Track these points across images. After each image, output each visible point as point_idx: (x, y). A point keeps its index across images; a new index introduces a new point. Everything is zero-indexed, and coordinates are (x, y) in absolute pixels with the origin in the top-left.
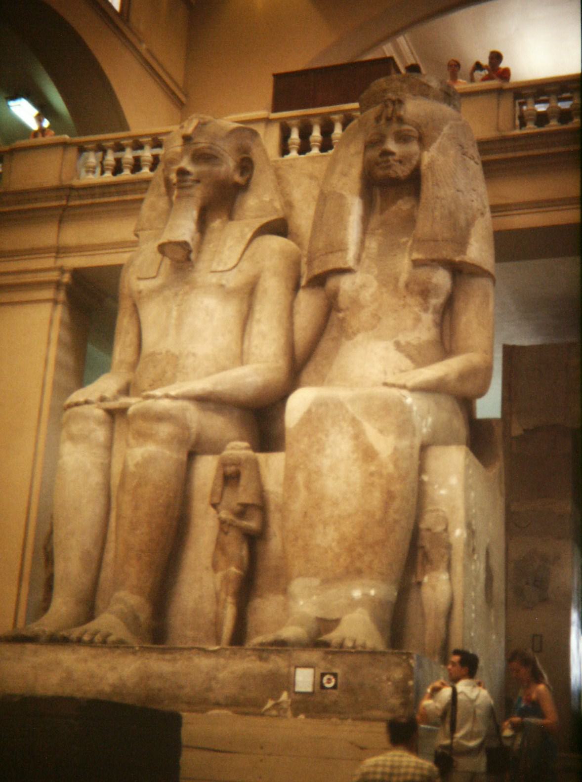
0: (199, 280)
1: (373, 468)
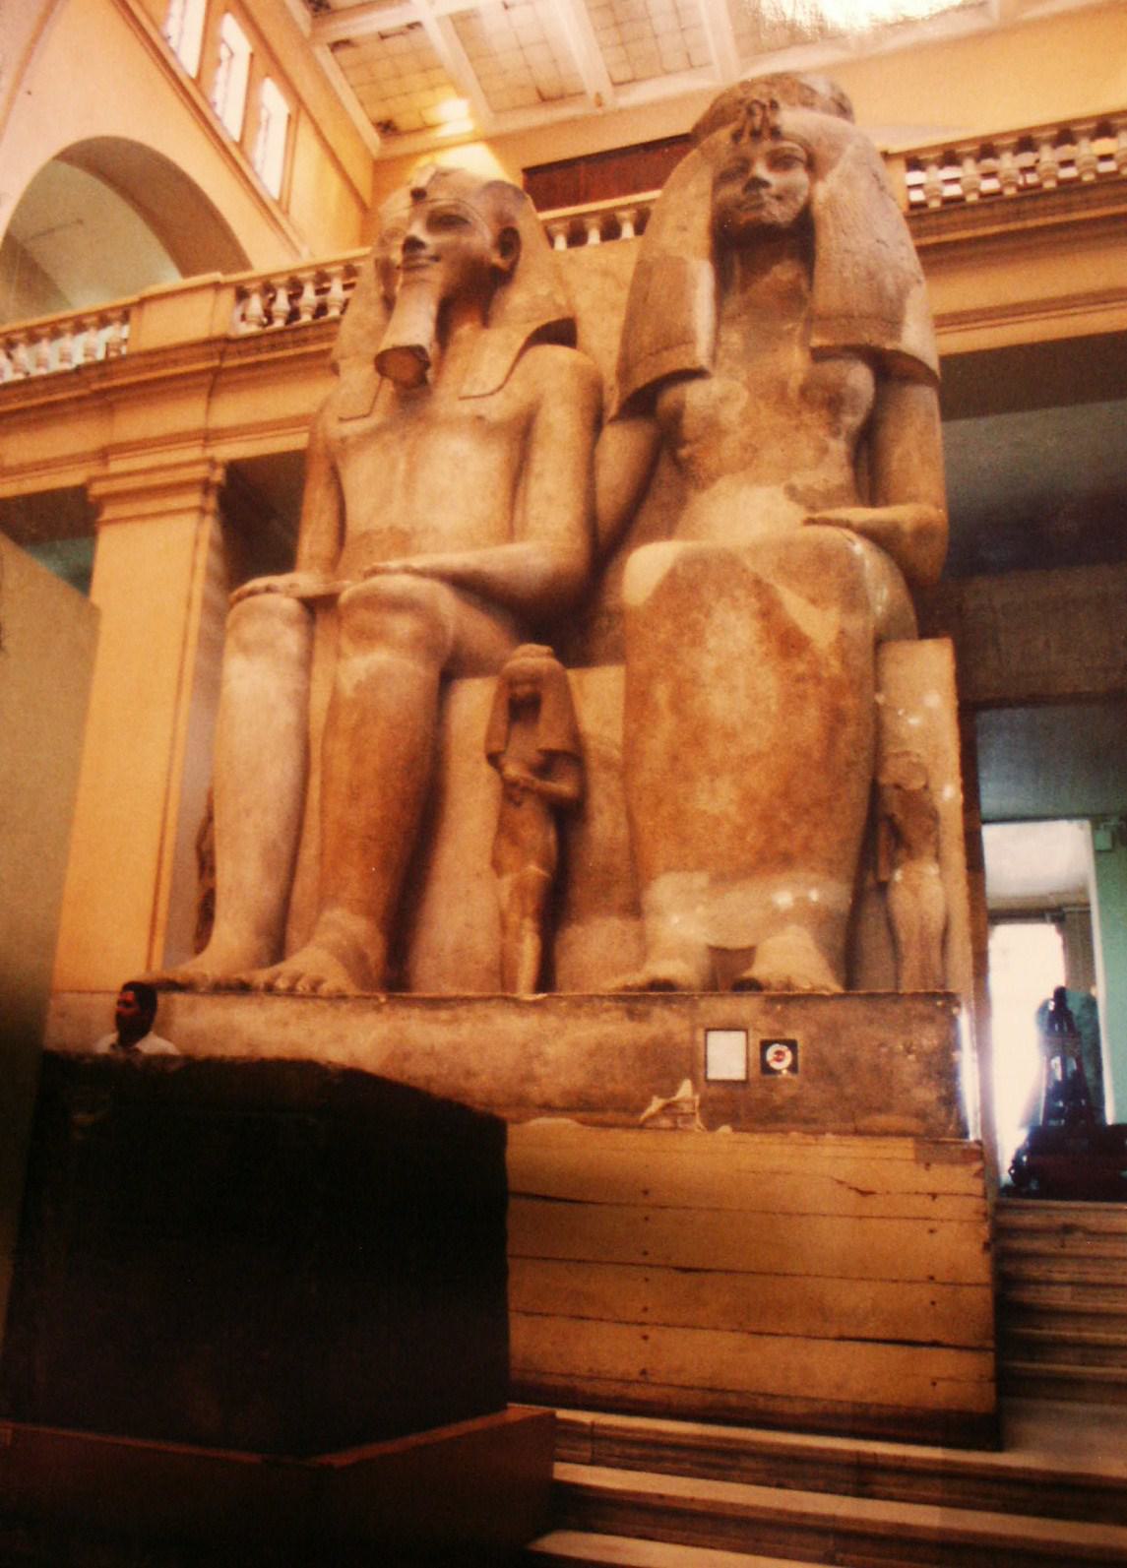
0: (442, 411)
1: (801, 667)
